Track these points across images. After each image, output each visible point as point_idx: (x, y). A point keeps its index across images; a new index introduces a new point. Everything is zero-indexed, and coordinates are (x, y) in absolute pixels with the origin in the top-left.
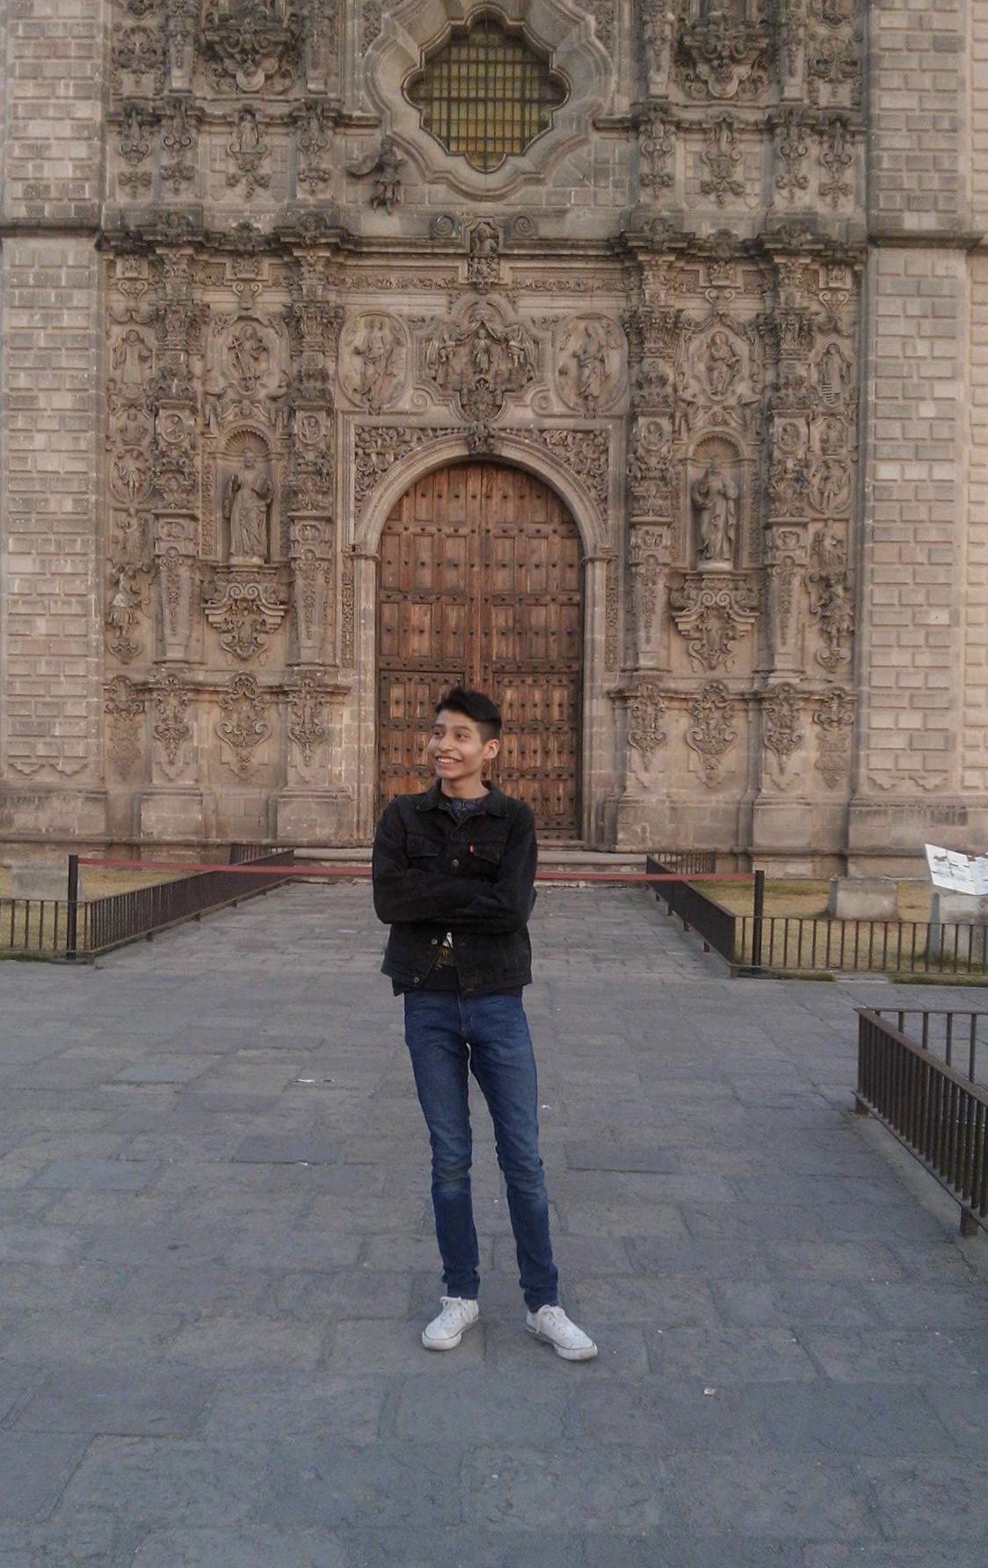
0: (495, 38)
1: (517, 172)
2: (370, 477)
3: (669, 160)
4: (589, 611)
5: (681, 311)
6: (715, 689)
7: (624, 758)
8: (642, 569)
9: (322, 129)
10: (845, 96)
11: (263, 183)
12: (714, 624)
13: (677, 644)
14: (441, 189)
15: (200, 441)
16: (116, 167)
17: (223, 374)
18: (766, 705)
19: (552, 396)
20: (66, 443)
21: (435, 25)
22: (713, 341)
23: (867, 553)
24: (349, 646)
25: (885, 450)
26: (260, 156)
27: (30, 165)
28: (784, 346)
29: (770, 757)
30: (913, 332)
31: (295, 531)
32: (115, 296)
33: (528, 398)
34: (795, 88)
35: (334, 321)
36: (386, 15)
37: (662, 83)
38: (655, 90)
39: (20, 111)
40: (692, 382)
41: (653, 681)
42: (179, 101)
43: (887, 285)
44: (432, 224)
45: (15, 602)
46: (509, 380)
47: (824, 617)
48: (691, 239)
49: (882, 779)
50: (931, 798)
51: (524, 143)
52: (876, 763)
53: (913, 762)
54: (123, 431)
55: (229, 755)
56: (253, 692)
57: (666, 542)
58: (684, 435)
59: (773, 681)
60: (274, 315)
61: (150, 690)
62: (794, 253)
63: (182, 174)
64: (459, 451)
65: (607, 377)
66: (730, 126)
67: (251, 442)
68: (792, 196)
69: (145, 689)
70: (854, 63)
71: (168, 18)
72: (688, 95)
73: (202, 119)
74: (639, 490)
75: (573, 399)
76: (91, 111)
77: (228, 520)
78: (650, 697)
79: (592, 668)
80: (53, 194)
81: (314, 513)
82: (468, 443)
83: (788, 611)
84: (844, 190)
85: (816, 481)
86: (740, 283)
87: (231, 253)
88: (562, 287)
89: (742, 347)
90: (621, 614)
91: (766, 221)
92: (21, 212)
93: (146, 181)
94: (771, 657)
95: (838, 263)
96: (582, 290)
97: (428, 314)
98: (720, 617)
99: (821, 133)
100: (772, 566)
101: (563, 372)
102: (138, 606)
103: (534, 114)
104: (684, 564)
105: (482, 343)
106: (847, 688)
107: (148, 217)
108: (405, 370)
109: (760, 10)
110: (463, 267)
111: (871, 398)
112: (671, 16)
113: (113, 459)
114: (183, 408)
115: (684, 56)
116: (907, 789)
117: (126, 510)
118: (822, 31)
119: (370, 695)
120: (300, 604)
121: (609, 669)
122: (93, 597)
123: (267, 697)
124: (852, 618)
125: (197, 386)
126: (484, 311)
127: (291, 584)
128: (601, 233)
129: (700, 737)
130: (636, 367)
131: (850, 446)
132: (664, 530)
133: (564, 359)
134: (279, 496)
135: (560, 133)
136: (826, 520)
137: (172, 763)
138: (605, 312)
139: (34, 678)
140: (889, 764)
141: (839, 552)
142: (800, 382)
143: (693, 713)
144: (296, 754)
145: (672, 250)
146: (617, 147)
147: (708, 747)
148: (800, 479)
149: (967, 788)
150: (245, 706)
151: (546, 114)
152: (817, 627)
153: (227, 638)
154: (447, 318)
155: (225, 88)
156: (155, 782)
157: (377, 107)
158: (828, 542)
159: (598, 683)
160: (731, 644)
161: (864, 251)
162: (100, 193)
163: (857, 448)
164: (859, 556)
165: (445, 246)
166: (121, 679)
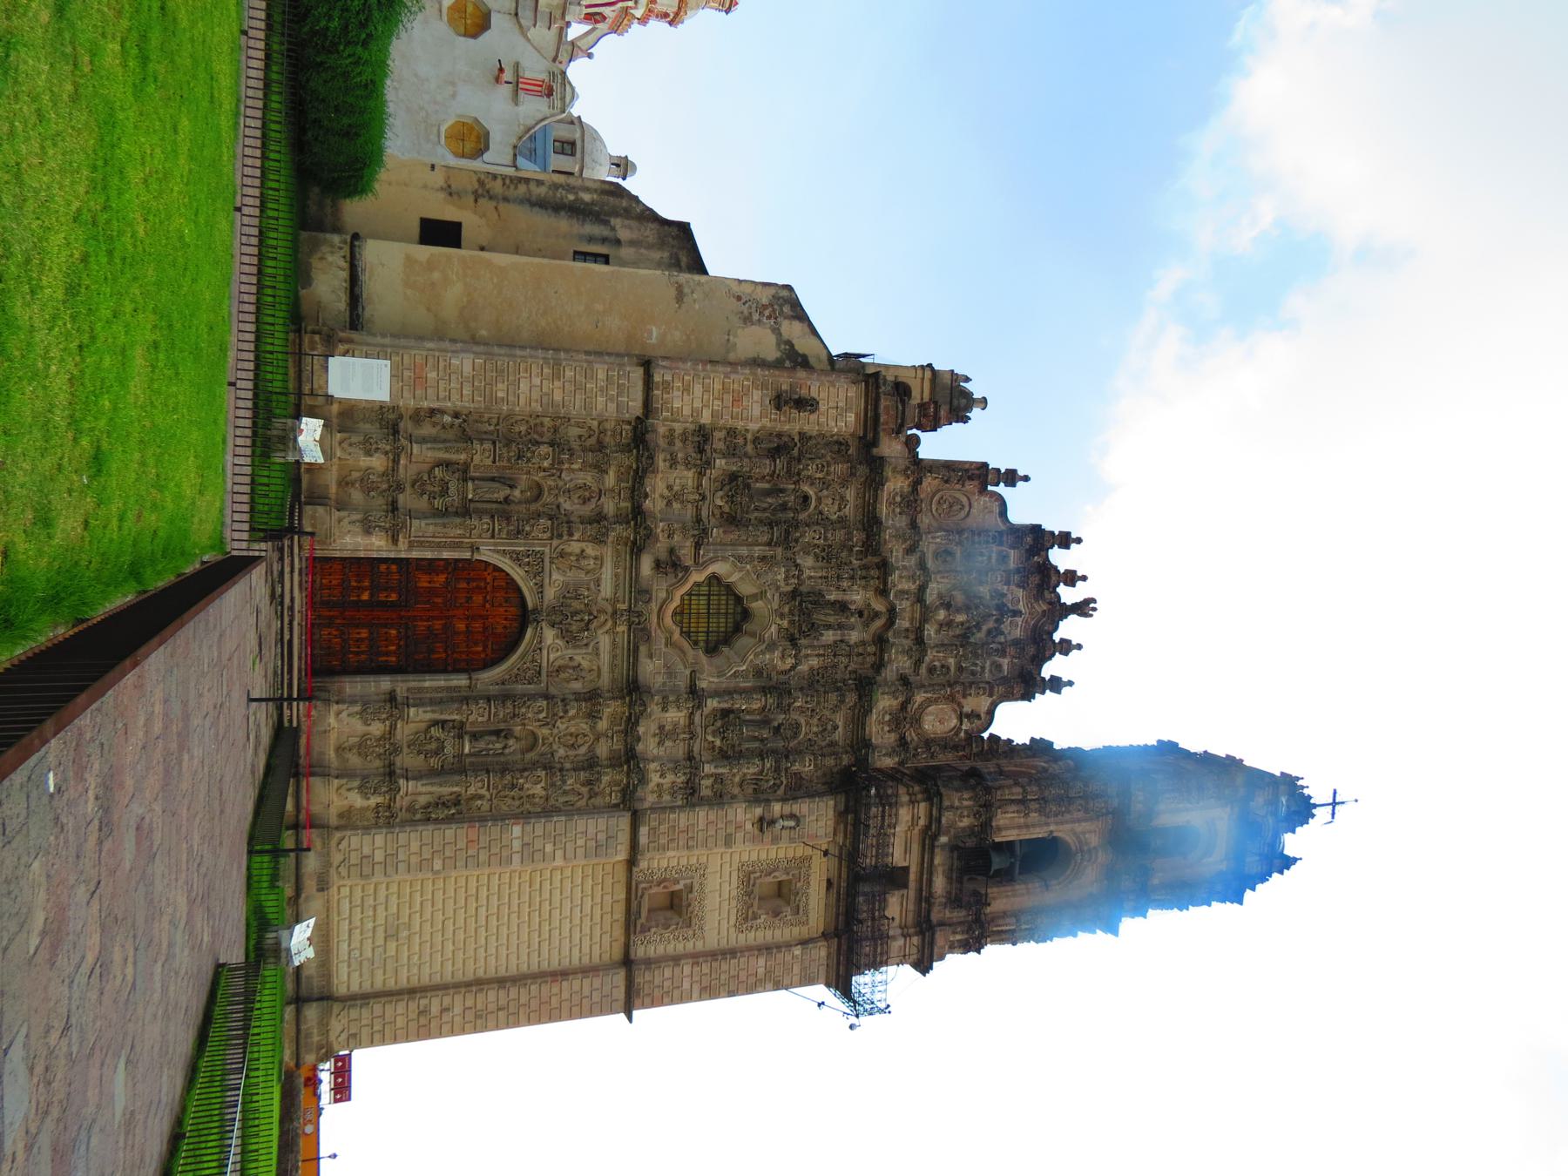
0: (739, 617)
1: (671, 633)
2: (517, 558)
3: (675, 710)
4: (442, 677)
5: (601, 718)
6: (396, 750)
7: (356, 702)
8: (465, 707)
9: (694, 536)
10: (706, 792)
11: (669, 503)
12: (434, 746)
13: (423, 726)
14: (663, 595)
15: (536, 466)
17: (571, 480)
18: (387, 779)
19: (559, 653)
20: (535, 395)
21: (745, 589)
22: (585, 736)
23: (472, 824)
24: (421, 545)
25: (529, 828)
26: (682, 502)
27: (680, 384)
28: (582, 773)
29: (356, 783)
30: (589, 837)
31: (486, 519)
32: (613, 423)
33: (557, 641)
34: (708, 769)
35: (599, 540)
36: (748, 566)
37: (712, 704)
38: (709, 701)
39: (707, 381)
40: (565, 726)
41: (401, 717)
42: (709, 464)
43: (613, 821)
44: (647, 592)
45: (445, 360)
46: (567, 631)
47: (437, 804)
48: (637, 723)
49: (344, 843)
50: (333, 871)
51: (686, 634)
52: (355, 840)
53: (355, 858)
54: (542, 424)
55: (355, 475)
56: (394, 491)
57: (480, 719)
58: (538, 724)
59: (402, 782)
60: (602, 508)
61: (394, 435)
62: (628, 775)
63: (673, 463)
64: (530, 605)
65: (568, 682)
66: (691, 738)
67: (536, 492)
68: (656, 772)
69: (396, 432)
70: (721, 796)
71: (750, 458)
72: (707, 717)
73: (701, 474)
74: (509, 704)
75: (557, 664)
76: (706, 418)
77: (493, 479)
78: (392, 715)
79: (409, 681)
80: (665, 396)
81: (497, 529)
82: (535, 610)
83: (441, 786)
84: (660, 796)
85: (512, 793)
86: (615, 747)
87: (634, 486)
88: (615, 657)
89: (583, 750)
90: (440, 695)
91: (645, 760)
92: (657, 378)
93: (671, 443)
94: (415, 778)
95: (624, 796)
96: (613, 666)
97: (602, 588)
98: (438, 748)
99: (687, 783)
100: (466, 776)
101: (571, 658)
102: (444, 427)
103: (702, 637)
104: (468, 728)
105: (586, 618)
106: (398, 820)
107: (652, 445)
108: (572, 576)
109: (747, 749)
110: (624, 606)
111: (555, 819)
112: (744, 707)
113: (526, 418)
114: (553, 460)
115: (725, 713)
116: (337, 858)
117: (498, 424)
118: (737, 779)
119: (392, 555)
120: (446, 520)
121: (408, 690)
122: (449, 404)
123: (390, 499)
124: (436, 819)
125: (566, 466)
126: (602, 618)
127: (456, 514)
128: (641, 678)
129: (368, 742)
130: (572, 697)
131: (531, 810)
132: (485, 719)
133: (578, 659)
134: (506, 507)
135: (690, 652)
136: (491, 800)
137: (351, 445)
138: (601, 681)
139: (400, 368)
140: (352, 847)
141: (474, 808)
142: (564, 782)
143: (382, 738)
144: (357, 516)
145: (631, 714)
146: (682, 683)
147: (362, 747)
148: (513, 786)
149: (339, 889)
150: (385, 486)
151: (702, 644)
152: (431, 800)
153: (425, 478)
154: (599, 598)
155: (716, 484)
156: (339, 435)
157: (706, 562)
158: (479, 802)
159: (400, 684)
160: (422, 756)
161: (629, 809)
162: (666, 419)
163: (529, 813)
164: (471, 820)
165: (635, 598)
166: (401, 417)
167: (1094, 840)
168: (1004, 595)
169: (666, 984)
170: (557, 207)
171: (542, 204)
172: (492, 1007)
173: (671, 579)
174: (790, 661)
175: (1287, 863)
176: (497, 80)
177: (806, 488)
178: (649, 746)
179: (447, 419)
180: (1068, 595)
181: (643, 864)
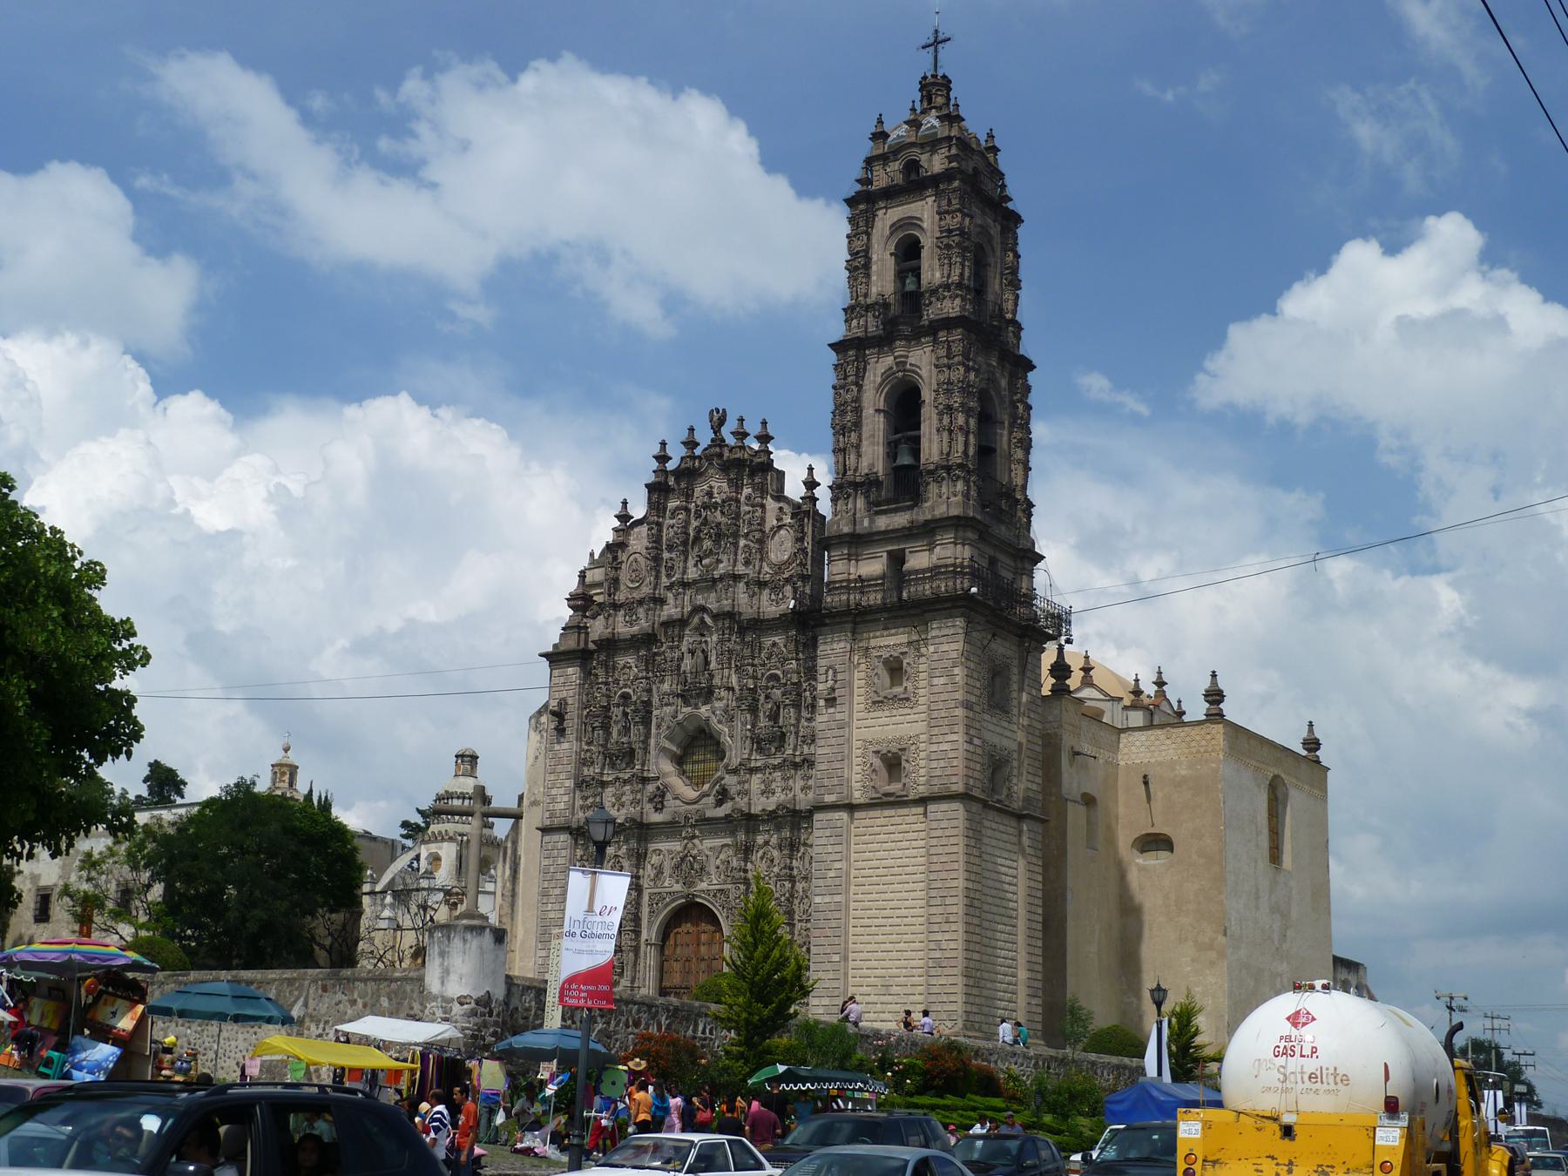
16: (579, 802)
76: (570, 783)
84: (810, 788)
92: (548, 822)
101: (718, 868)
162: (573, 814)
167: (889, 361)
168: (697, 506)
169: (942, 764)
170: (514, 894)
171: (513, 905)
172: (940, 910)
173: (668, 796)
174: (723, 693)
177: (616, 700)
178: (771, 804)
180: (704, 437)
181: (858, 797)
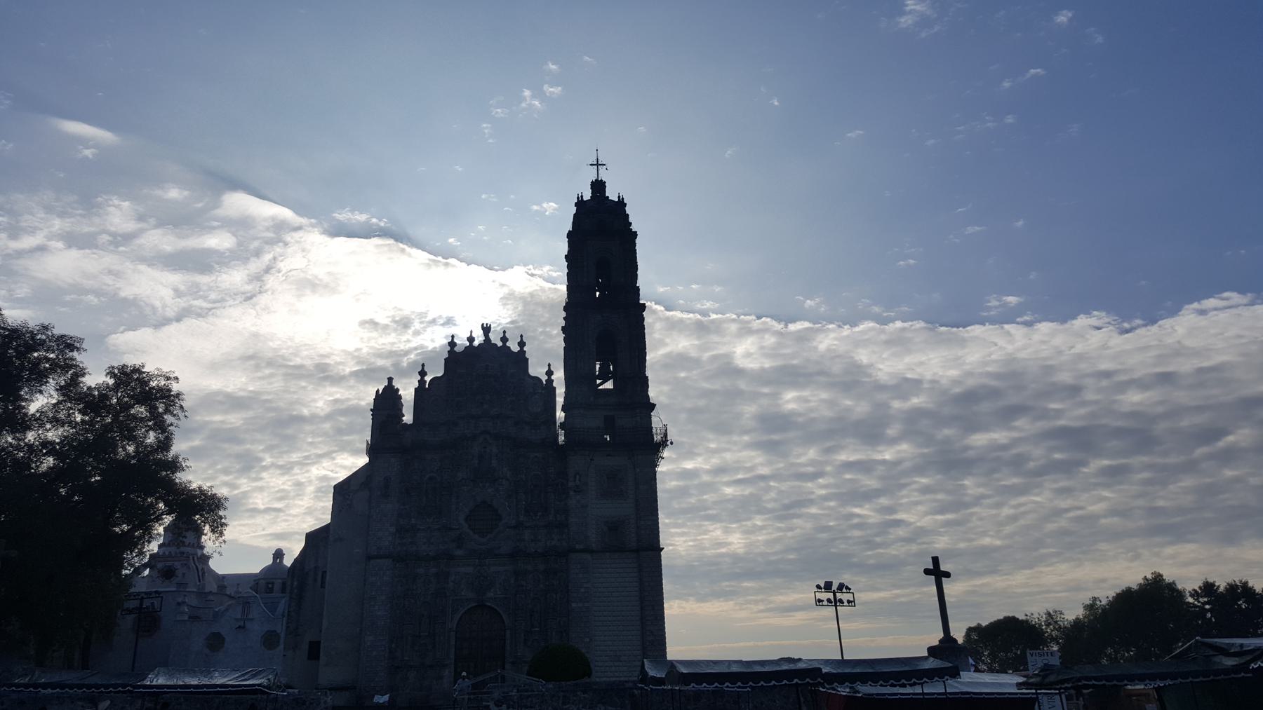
33: (492, 591)
76: (393, 529)
112: (524, 503)
175: (621, 204)
176: (244, 627)
179: (393, 646)
180: (479, 339)
